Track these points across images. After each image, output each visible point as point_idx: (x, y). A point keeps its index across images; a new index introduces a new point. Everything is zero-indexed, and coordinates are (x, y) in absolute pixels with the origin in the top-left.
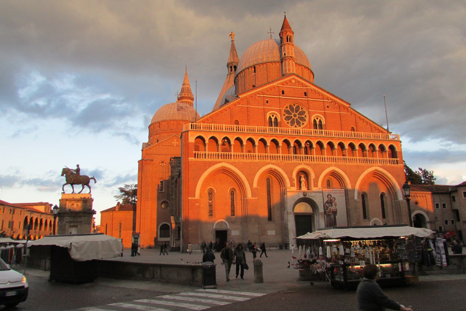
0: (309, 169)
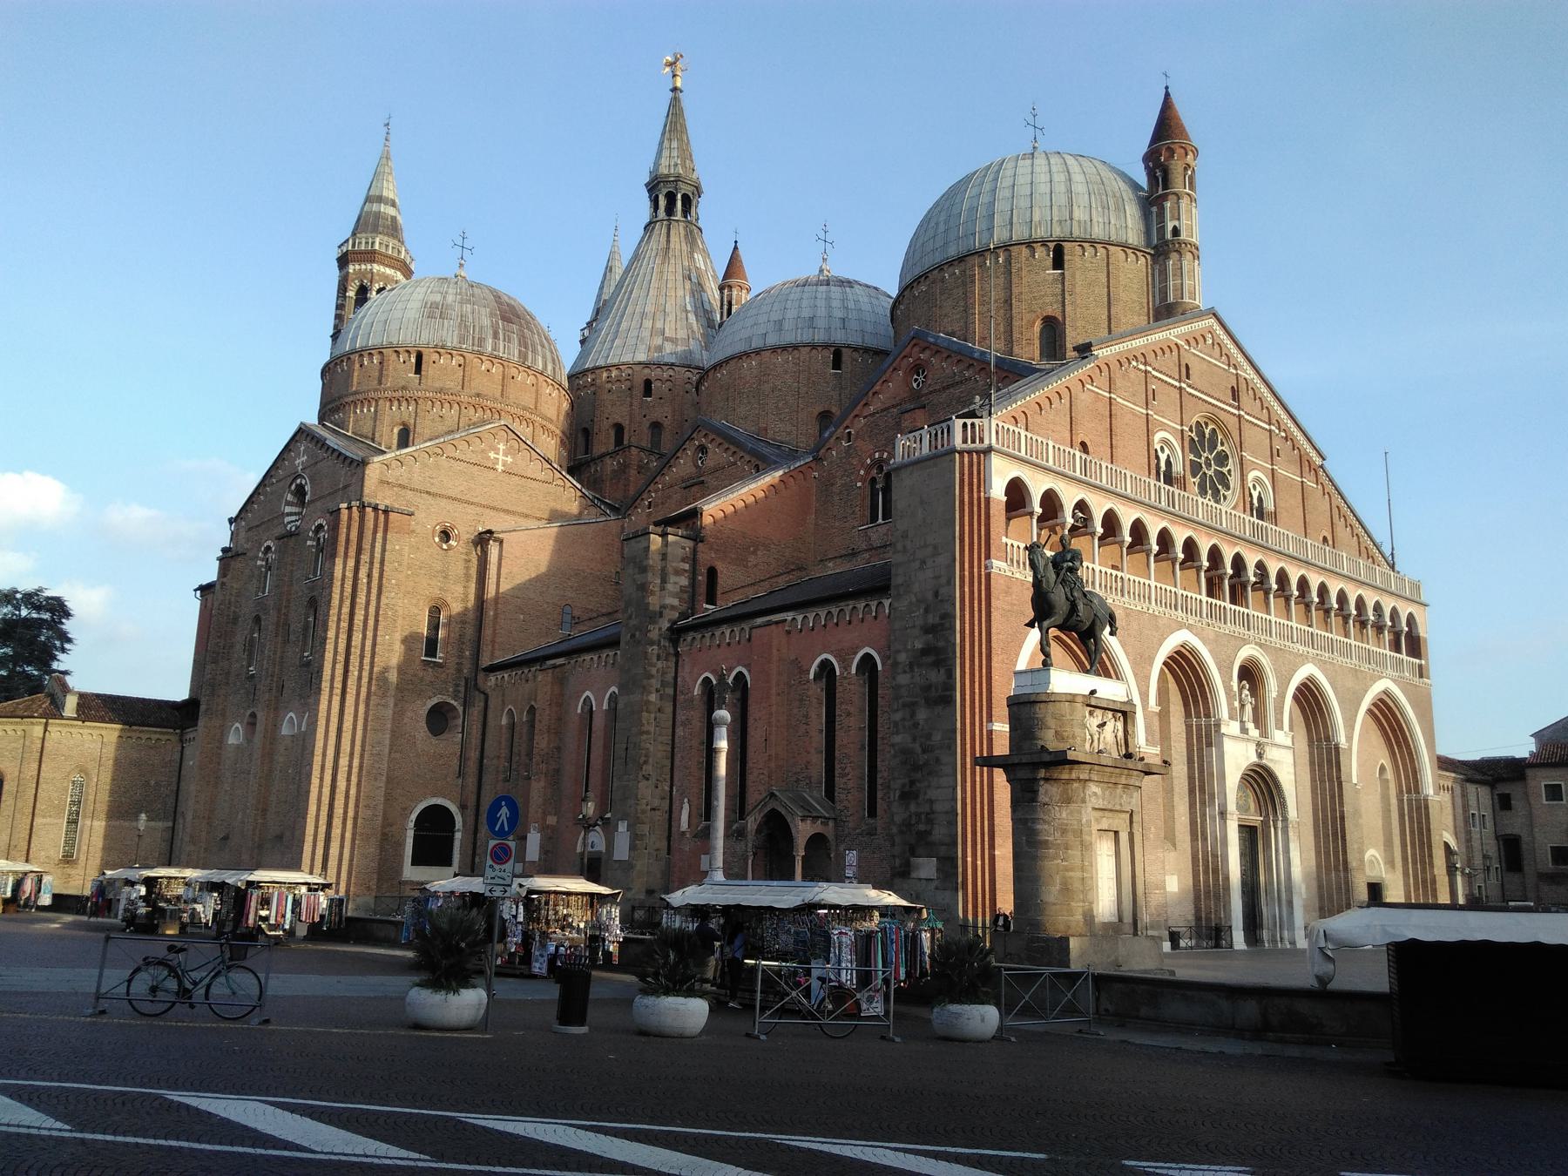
0: (1265, 661)
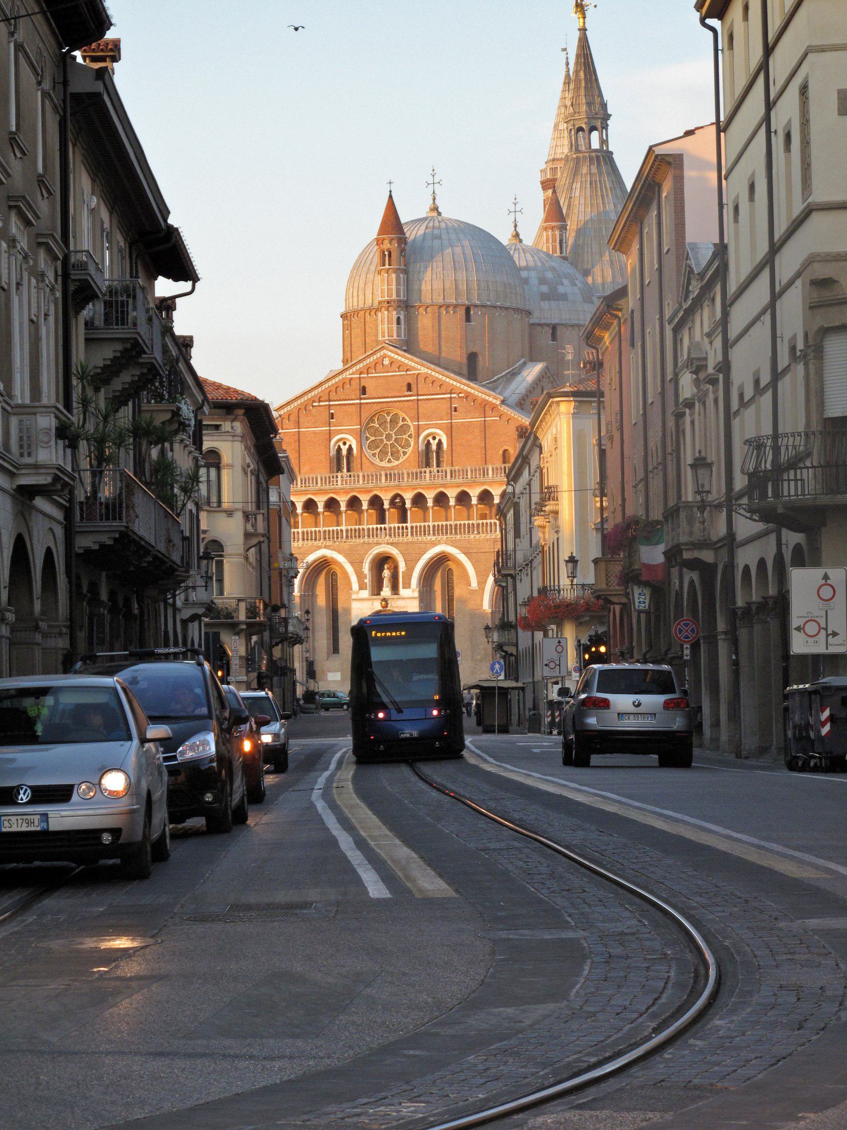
0: (394, 552)
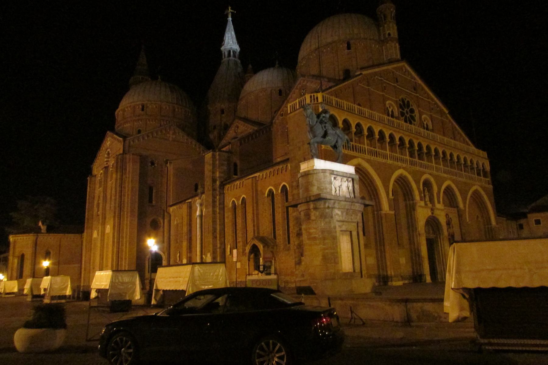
0: (432, 180)
